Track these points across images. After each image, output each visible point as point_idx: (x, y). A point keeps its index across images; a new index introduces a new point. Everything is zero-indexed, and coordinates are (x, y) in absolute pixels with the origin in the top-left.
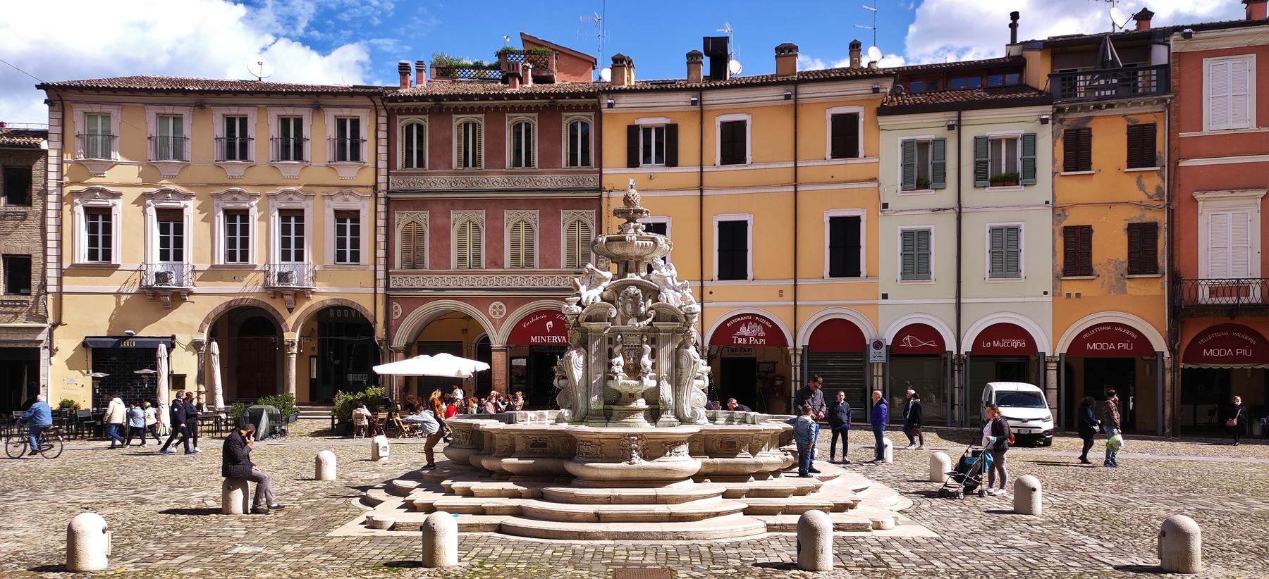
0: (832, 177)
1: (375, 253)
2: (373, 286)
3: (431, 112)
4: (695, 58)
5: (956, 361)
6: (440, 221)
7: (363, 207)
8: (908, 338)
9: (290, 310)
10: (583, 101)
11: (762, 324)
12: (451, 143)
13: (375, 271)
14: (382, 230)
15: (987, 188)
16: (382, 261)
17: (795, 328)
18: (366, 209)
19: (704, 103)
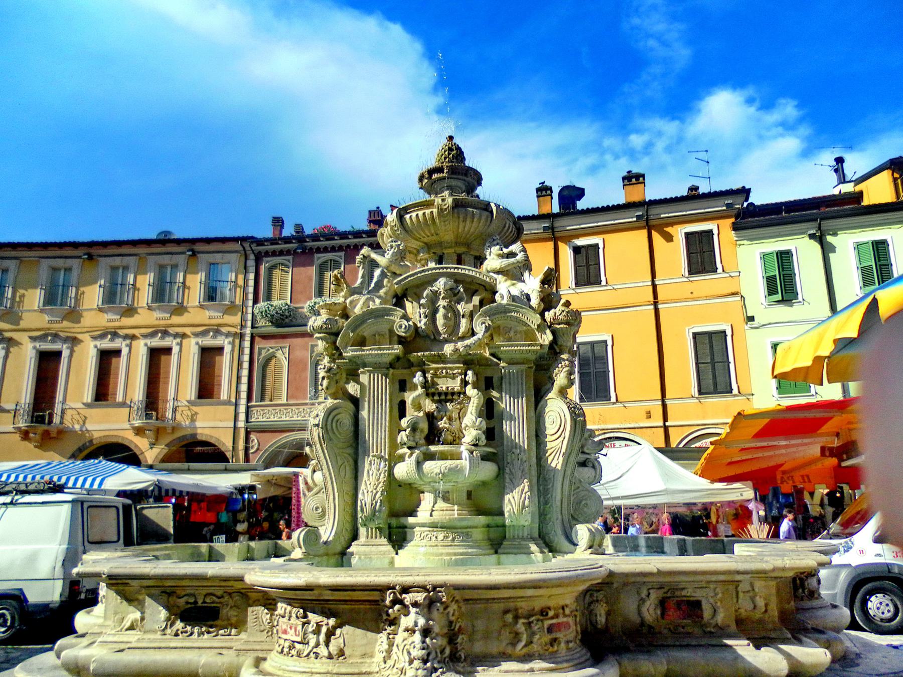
3: (294, 253)
16: (244, 395)
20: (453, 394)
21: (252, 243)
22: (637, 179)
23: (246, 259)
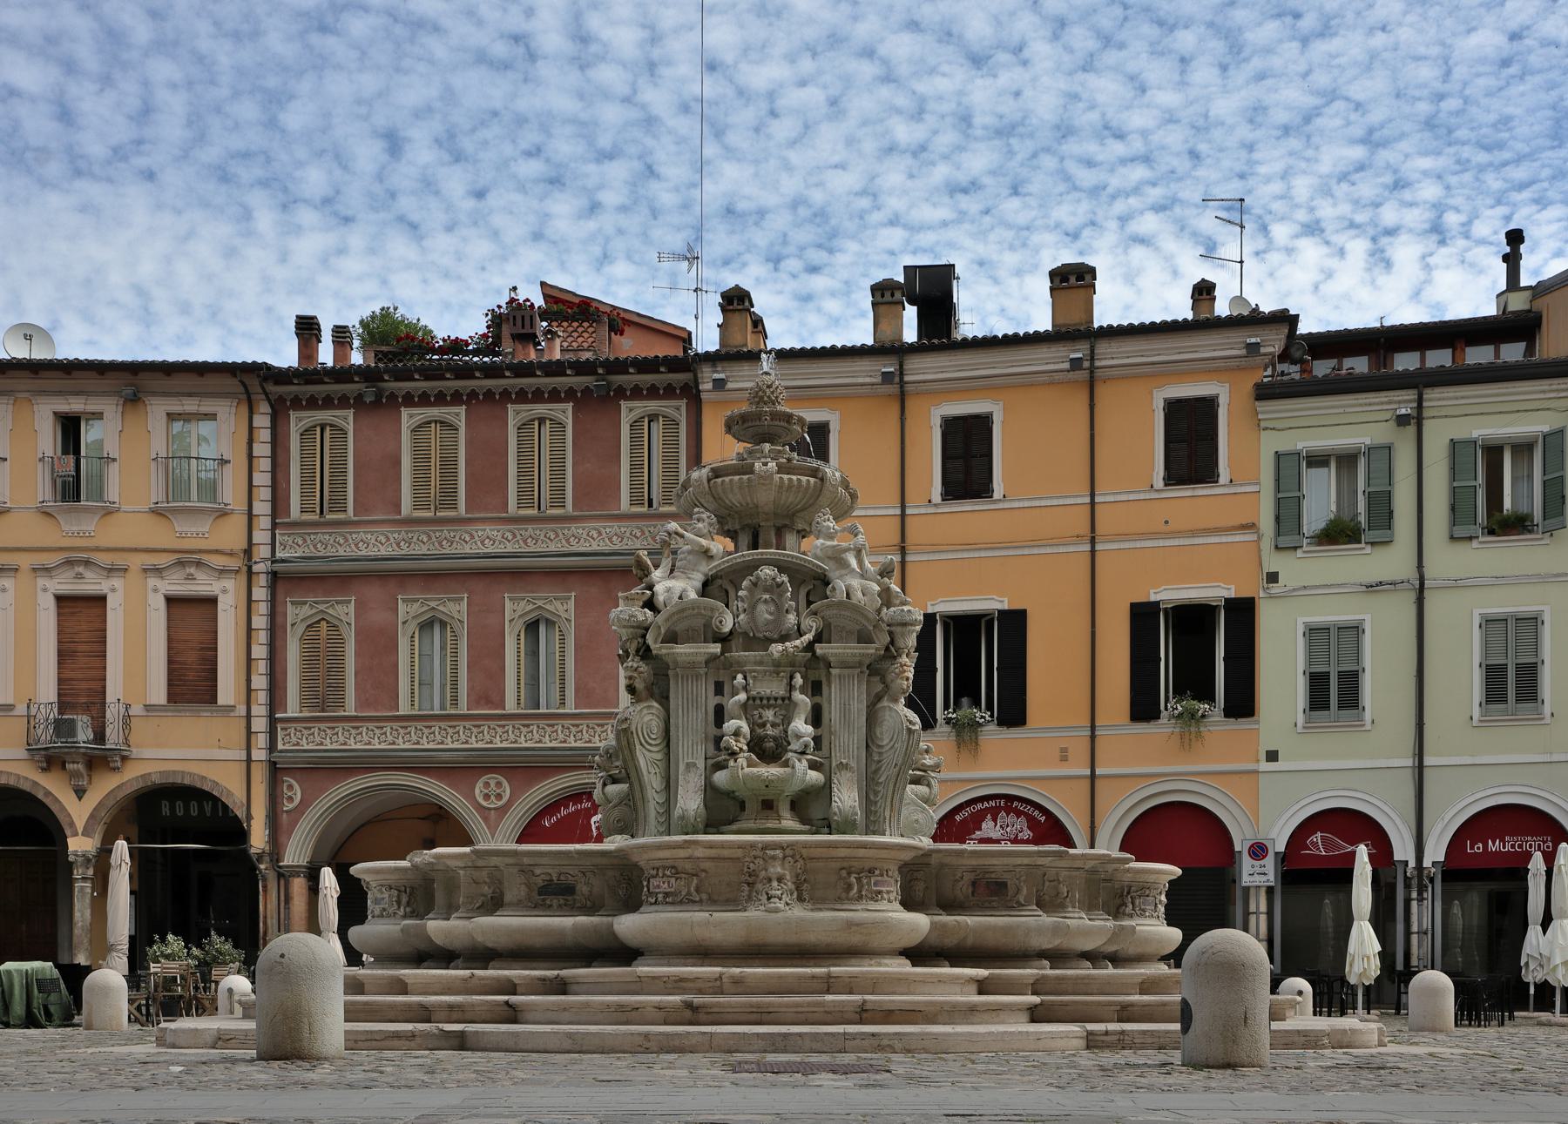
0: (1167, 522)
2: (244, 746)
3: (358, 403)
4: (888, 294)
5: (1415, 882)
6: (378, 617)
8: (1317, 837)
9: (80, 793)
10: (662, 378)
11: (1026, 815)
12: (397, 463)
15: (1475, 544)
17: (1093, 822)
19: (907, 378)
20: (776, 699)
21: (265, 379)
22: (1080, 278)
23: (251, 413)
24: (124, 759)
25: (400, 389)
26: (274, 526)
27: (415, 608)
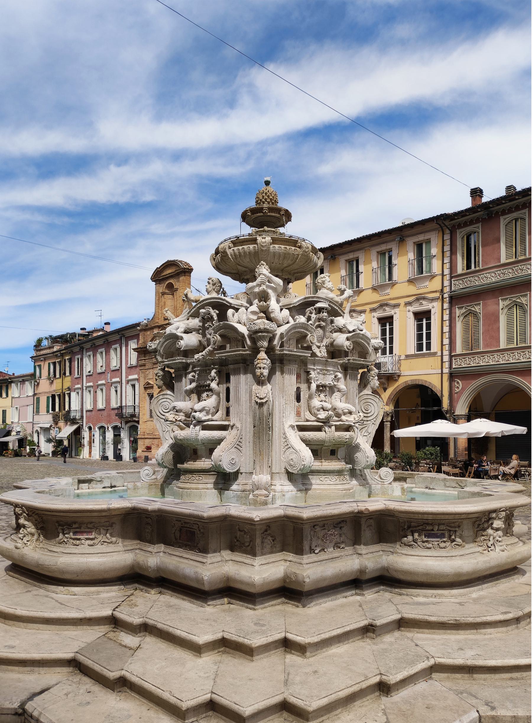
1: (442, 341)
2: (440, 368)
7: (433, 307)
13: (442, 356)
14: (447, 323)
16: (447, 347)
18: (435, 308)
23: (443, 234)
24: (399, 376)
25: (500, 208)
26: (451, 277)
27: (507, 302)
